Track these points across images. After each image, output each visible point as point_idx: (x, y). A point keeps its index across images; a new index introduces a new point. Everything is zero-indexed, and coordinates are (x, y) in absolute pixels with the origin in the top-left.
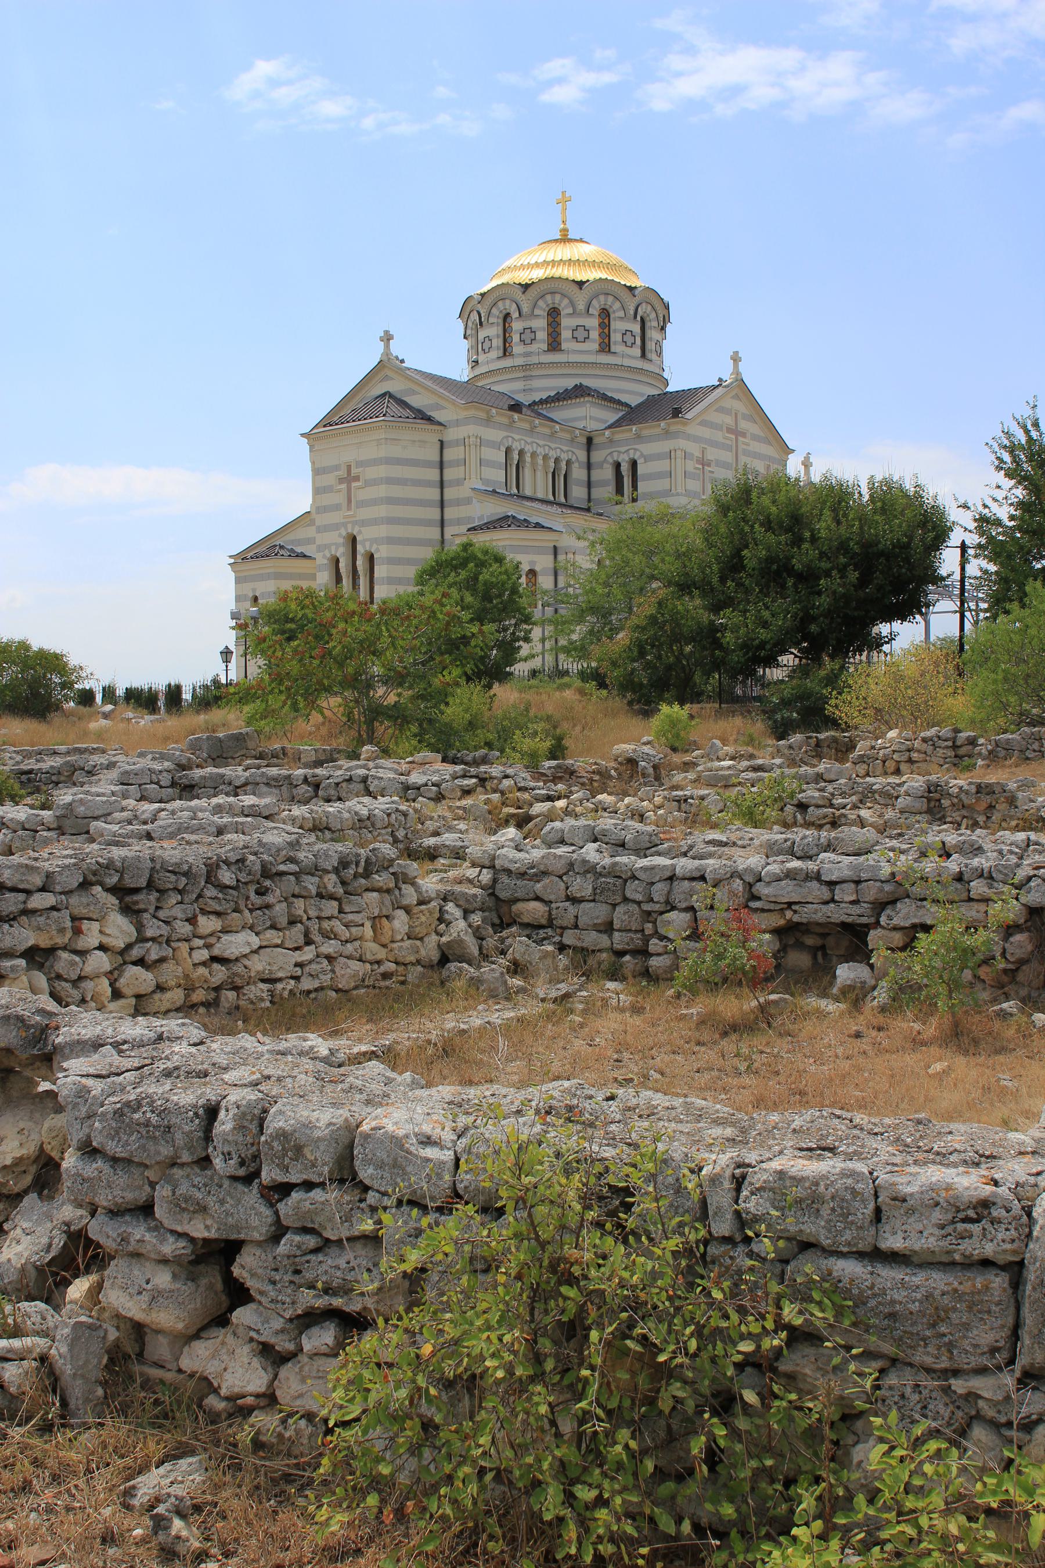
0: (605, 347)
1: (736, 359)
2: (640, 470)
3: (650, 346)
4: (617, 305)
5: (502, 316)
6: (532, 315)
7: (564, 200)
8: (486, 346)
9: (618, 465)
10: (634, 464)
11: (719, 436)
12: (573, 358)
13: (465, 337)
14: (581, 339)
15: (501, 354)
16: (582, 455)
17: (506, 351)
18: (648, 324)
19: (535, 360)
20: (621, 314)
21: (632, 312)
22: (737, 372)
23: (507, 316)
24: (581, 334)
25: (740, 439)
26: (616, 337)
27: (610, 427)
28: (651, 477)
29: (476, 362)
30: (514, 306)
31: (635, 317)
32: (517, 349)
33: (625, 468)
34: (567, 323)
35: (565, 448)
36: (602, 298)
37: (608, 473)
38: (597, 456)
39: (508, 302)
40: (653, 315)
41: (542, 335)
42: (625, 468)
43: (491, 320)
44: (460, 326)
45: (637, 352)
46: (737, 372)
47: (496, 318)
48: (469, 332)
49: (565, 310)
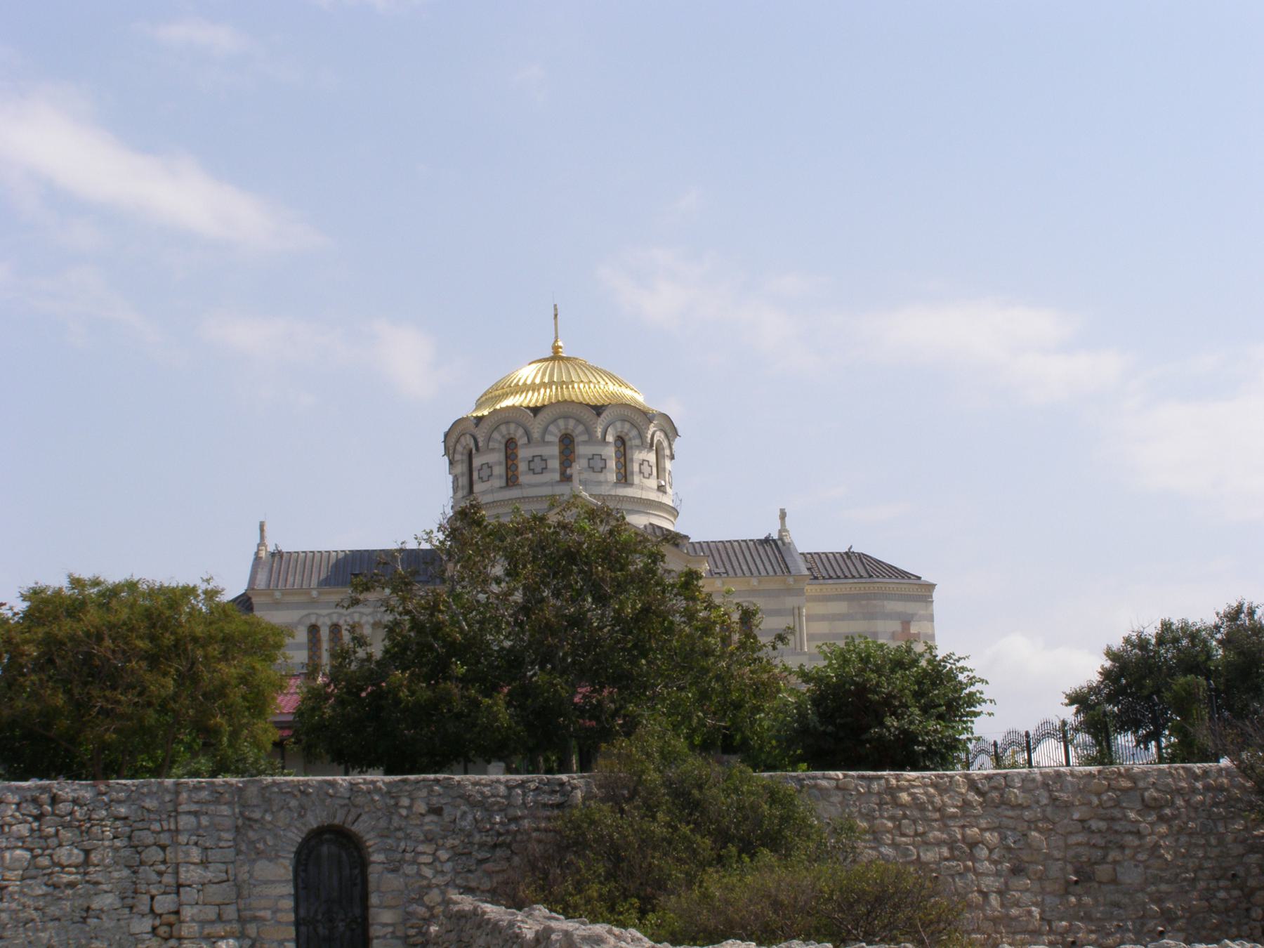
1: (783, 515)
4: (665, 444)
8: (538, 465)
12: (645, 495)
14: (646, 475)
20: (667, 452)
22: (783, 530)
23: (567, 442)
24: (646, 468)
30: (581, 428)
34: (639, 456)
36: (658, 433)
39: (572, 423)
41: (612, 464)
43: (548, 438)
46: (783, 530)
47: (553, 437)
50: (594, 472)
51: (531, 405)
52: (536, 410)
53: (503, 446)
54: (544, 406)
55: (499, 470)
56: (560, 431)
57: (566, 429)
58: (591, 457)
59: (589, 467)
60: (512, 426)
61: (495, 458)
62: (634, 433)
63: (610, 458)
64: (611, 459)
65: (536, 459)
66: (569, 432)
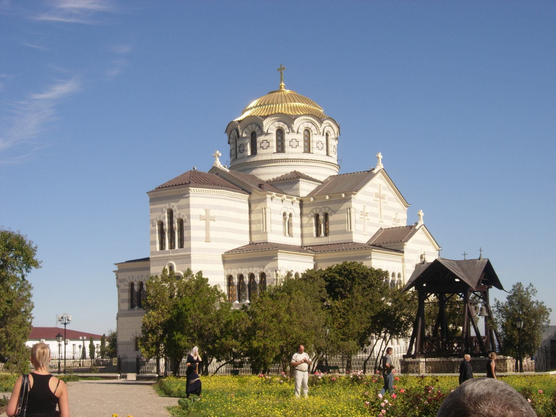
0: (308, 149)
2: (331, 219)
3: (331, 149)
4: (313, 128)
5: (250, 133)
6: (267, 134)
7: (281, 69)
8: (241, 149)
9: (317, 217)
10: (326, 216)
11: (371, 199)
13: (229, 143)
14: (294, 146)
15: (249, 153)
16: (296, 210)
17: (254, 152)
18: (330, 137)
19: (269, 157)
21: (321, 131)
24: (294, 143)
25: (382, 200)
26: (313, 145)
27: (311, 194)
28: (337, 222)
29: (237, 158)
30: (257, 128)
31: (323, 135)
32: (259, 151)
33: (321, 217)
34: (288, 137)
35: (288, 207)
37: (313, 221)
38: (306, 210)
39: (254, 125)
40: (332, 132)
41: (274, 144)
42: (321, 217)
44: (226, 137)
45: (325, 153)
48: (231, 141)
49: (286, 130)
50: (263, 149)
51: (240, 120)
52: (240, 122)
53: (234, 141)
54: (243, 119)
55: (233, 152)
56: (250, 131)
57: (253, 129)
58: (268, 141)
59: (261, 147)
60: (235, 130)
61: (233, 146)
62: (285, 127)
63: (272, 141)
64: (272, 141)
65: (264, 141)
66: (254, 130)
